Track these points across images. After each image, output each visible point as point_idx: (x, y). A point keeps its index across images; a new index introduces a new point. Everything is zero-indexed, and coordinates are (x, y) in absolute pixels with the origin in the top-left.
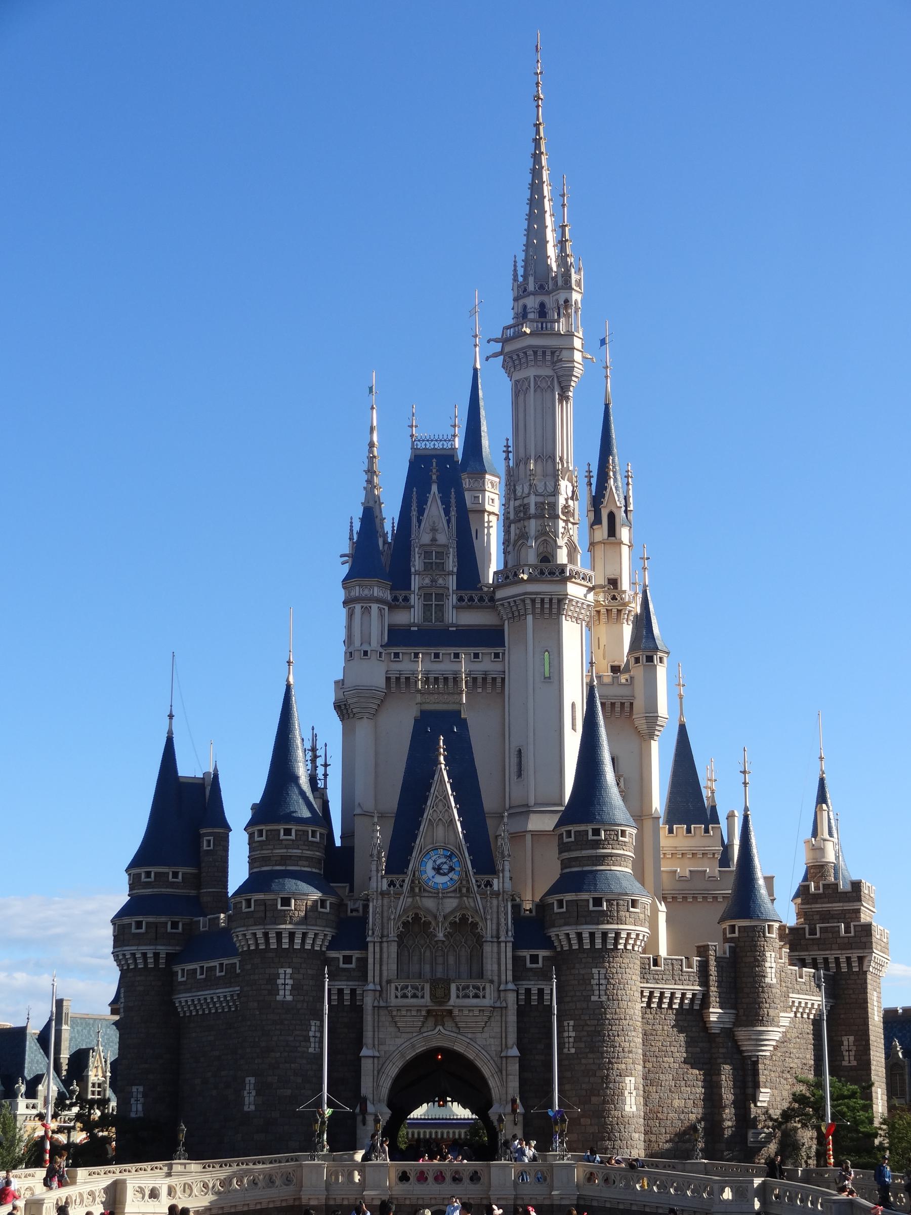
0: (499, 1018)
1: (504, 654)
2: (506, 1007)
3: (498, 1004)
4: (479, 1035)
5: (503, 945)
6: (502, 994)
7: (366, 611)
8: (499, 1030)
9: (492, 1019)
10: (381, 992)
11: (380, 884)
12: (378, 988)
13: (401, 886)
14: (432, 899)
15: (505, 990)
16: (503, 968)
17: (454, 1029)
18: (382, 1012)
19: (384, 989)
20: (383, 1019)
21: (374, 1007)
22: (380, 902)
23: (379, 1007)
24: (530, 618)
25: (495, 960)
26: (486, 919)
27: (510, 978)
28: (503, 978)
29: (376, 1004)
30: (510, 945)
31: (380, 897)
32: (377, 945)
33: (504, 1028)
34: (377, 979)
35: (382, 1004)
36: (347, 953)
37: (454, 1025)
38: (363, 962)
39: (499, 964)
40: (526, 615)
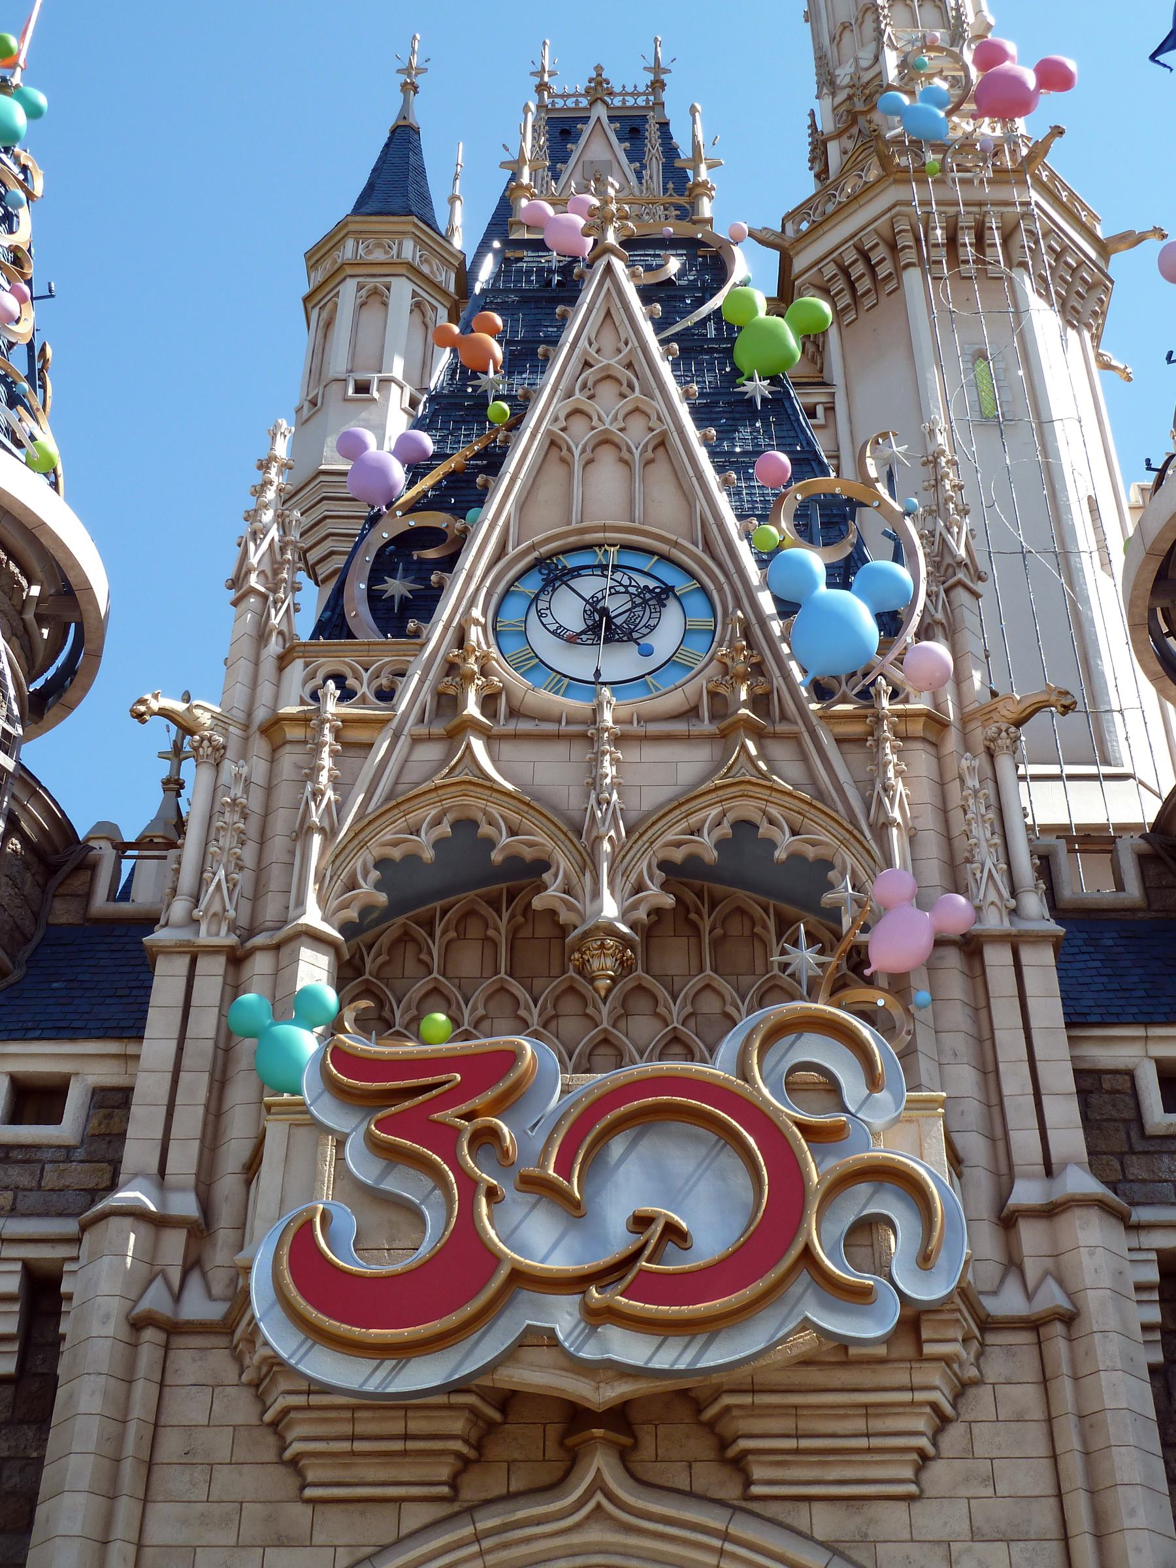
0: (1027, 1396)
1: (830, 409)
2: (1069, 1319)
3: (1009, 1302)
4: (893, 1517)
5: (997, 958)
6: (1030, 1235)
7: (377, 297)
8: (1030, 1478)
9: (981, 1402)
10: (200, 1230)
11: (266, 691)
12: (185, 1205)
13: (386, 695)
14: (559, 750)
15: (1050, 1212)
16: (1015, 1082)
17: (710, 1478)
18: (190, 1363)
19: (225, 1215)
20: (188, 1407)
21: (137, 1324)
22: (258, 768)
23: (173, 1329)
24: (912, 278)
25: (959, 1042)
26: (881, 829)
27: (1069, 1138)
28: (1025, 1142)
29: (156, 1300)
30: (1041, 965)
31: (260, 746)
32: (212, 970)
33: (1073, 1465)
34: (184, 1160)
35: (198, 1306)
36: (38, 1058)
37: (700, 1446)
38: (113, 1103)
39: (989, 1072)
40: (899, 270)
